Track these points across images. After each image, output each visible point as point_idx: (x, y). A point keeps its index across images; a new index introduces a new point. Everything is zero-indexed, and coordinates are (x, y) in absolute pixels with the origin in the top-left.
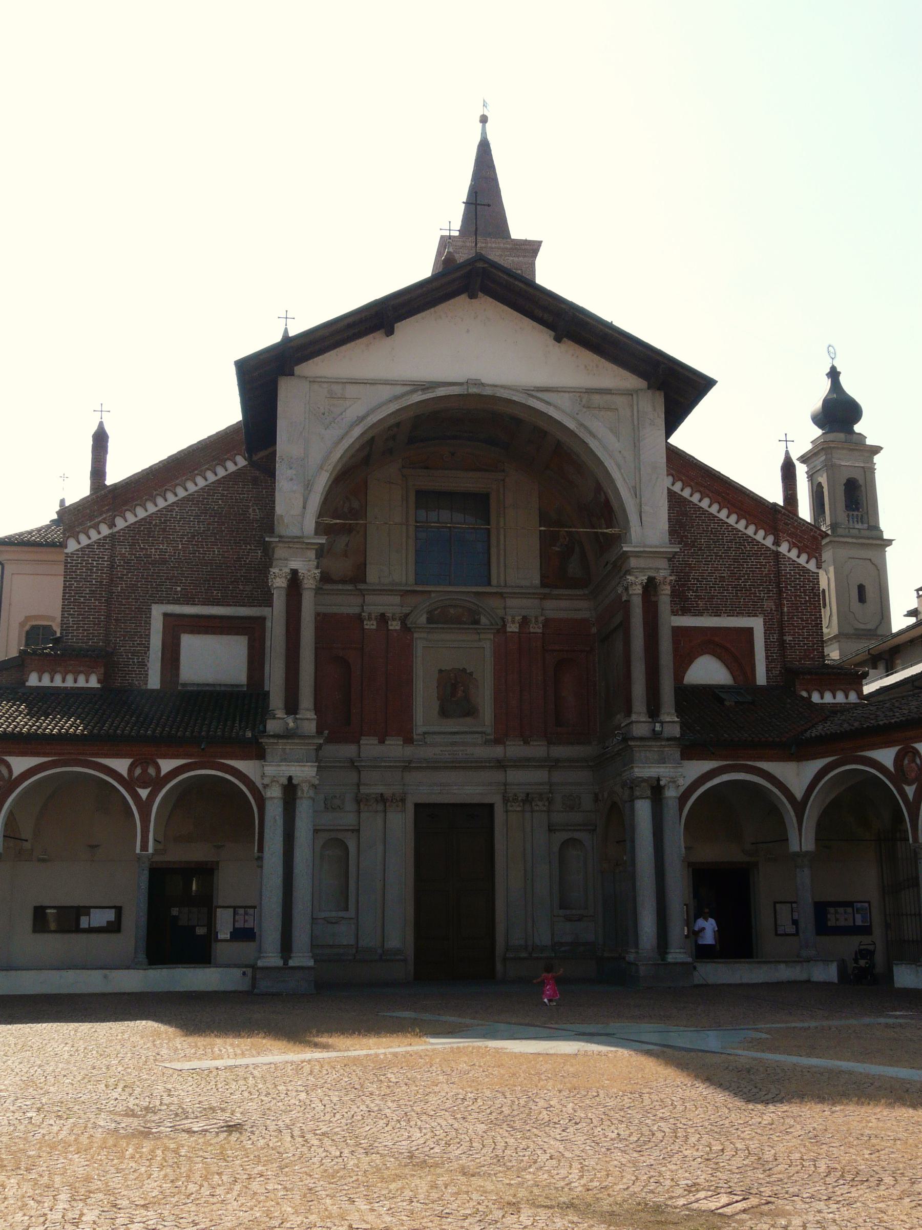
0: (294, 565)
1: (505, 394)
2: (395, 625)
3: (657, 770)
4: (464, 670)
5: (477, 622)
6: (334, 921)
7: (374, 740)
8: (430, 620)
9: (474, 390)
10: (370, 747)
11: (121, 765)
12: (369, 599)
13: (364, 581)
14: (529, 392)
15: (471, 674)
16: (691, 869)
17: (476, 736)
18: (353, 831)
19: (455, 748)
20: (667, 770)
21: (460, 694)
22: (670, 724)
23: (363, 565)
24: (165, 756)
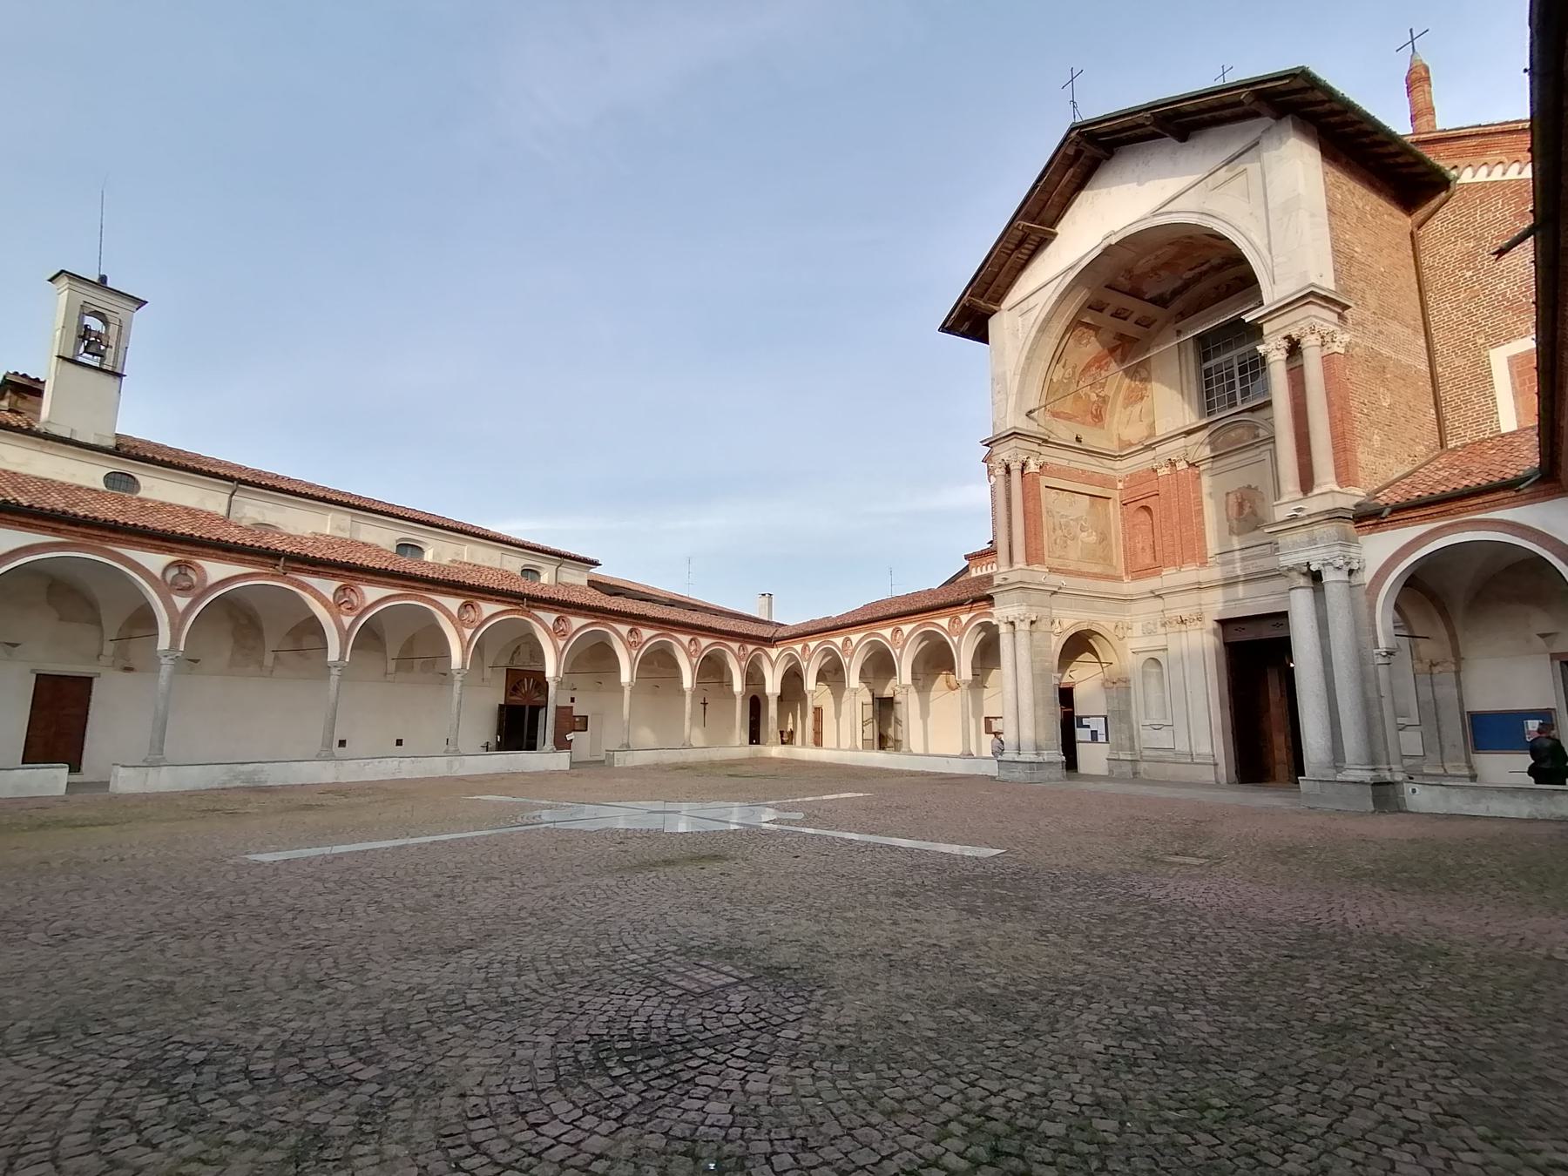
0: (1004, 456)
1: (1133, 230)
2: (1182, 465)
3: (1306, 554)
4: (1249, 487)
5: (1257, 436)
6: (1157, 727)
7: (1172, 570)
8: (1212, 450)
9: (1106, 243)
10: (1171, 577)
11: (944, 622)
12: (1159, 450)
13: (1152, 435)
14: (1155, 213)
15: (1256, 489)
16: (1557, 663)
17: (1264, 547)
18: (1163, 650)
19: (1246, 563)
20: (1320, 551)
21: (1247, 510)
22: (1320, 497)
23: (1152, 426)
24: (962, 613)
